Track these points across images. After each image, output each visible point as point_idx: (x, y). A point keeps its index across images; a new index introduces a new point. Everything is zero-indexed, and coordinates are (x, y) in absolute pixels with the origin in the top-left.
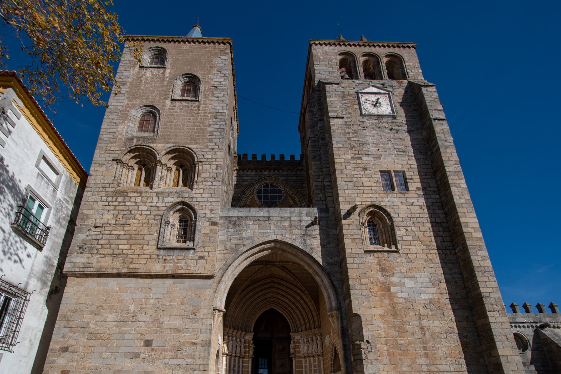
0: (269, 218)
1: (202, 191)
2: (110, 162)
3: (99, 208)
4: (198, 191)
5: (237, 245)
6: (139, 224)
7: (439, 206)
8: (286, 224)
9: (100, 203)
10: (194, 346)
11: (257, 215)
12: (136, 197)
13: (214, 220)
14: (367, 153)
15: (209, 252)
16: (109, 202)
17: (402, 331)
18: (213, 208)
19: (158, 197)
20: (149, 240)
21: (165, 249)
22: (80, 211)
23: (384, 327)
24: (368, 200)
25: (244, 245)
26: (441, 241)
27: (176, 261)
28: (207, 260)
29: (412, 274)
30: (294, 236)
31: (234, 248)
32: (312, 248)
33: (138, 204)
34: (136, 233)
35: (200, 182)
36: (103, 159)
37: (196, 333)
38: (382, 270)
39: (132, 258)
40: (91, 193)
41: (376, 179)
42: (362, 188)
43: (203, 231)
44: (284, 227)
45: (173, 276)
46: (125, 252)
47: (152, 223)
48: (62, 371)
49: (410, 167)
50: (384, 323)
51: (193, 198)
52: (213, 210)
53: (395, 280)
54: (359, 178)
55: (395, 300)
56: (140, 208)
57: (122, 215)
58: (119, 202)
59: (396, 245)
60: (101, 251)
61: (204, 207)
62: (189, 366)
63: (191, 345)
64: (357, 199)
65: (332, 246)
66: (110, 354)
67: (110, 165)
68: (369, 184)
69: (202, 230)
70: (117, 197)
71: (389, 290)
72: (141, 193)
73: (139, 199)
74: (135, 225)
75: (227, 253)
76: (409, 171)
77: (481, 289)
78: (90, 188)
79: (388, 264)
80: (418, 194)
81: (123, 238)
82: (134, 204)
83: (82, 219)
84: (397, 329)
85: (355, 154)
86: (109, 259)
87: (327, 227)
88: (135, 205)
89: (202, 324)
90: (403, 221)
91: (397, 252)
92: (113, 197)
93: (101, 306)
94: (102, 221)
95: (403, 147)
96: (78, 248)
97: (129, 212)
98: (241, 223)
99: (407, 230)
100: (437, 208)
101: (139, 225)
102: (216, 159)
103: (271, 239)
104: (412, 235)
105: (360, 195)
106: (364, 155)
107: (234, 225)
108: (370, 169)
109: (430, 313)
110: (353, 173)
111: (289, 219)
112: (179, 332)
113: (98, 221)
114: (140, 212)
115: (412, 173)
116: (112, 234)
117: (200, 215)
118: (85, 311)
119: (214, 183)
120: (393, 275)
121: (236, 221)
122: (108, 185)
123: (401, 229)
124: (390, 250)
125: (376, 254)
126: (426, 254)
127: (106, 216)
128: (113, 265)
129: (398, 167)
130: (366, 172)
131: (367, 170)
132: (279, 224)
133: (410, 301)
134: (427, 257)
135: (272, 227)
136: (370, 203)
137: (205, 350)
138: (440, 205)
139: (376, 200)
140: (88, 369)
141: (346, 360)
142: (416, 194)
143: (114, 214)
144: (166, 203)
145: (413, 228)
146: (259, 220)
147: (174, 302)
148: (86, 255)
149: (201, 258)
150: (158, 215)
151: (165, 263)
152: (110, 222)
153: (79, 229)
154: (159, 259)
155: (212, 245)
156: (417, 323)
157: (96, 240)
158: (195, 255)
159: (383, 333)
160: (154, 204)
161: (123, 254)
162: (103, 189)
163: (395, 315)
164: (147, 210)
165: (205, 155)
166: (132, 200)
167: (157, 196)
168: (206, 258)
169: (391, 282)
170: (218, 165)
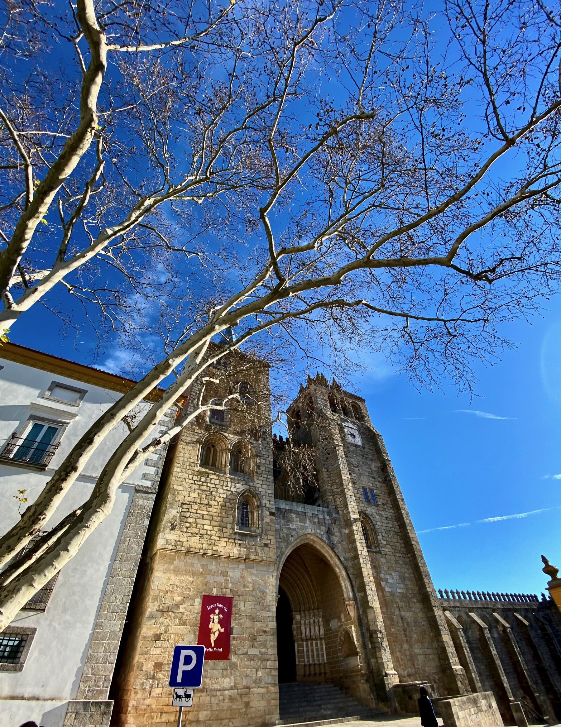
4: (259, 482)
5: (287, 535)
12: (215, 479)
15: (270, 540)
33: (217, 486)
34: (215, 514)
39: (215, 540)
46: (209, 532)
48: (155, 663)
51: (256, 487)
52: (270, 501)
53: (382, 576)
58: (203, 482)
59: (378, 546)
60: (190, 530)
62: (263, 656)
75: (281, 542)
83: (173, 494)
86: (196, 539)
89: (269, 611)
94: (189, 499)
113: (186, 498)
118: (174, 593)
119: (269, 477)
127: (192, 495)
128: (199, 546)
135: (308, 522)
138: (394, 518)
141: (364, 646)
147: (248, 587)
148: (177, 532)
149: (266, 545)
153: (170, 504)
154: (235, 543)
155: (272, 533)
157: (185, 517)
160: (228, 488)
161: (207, 534)
166: (213, 482)
168: (270, 546)
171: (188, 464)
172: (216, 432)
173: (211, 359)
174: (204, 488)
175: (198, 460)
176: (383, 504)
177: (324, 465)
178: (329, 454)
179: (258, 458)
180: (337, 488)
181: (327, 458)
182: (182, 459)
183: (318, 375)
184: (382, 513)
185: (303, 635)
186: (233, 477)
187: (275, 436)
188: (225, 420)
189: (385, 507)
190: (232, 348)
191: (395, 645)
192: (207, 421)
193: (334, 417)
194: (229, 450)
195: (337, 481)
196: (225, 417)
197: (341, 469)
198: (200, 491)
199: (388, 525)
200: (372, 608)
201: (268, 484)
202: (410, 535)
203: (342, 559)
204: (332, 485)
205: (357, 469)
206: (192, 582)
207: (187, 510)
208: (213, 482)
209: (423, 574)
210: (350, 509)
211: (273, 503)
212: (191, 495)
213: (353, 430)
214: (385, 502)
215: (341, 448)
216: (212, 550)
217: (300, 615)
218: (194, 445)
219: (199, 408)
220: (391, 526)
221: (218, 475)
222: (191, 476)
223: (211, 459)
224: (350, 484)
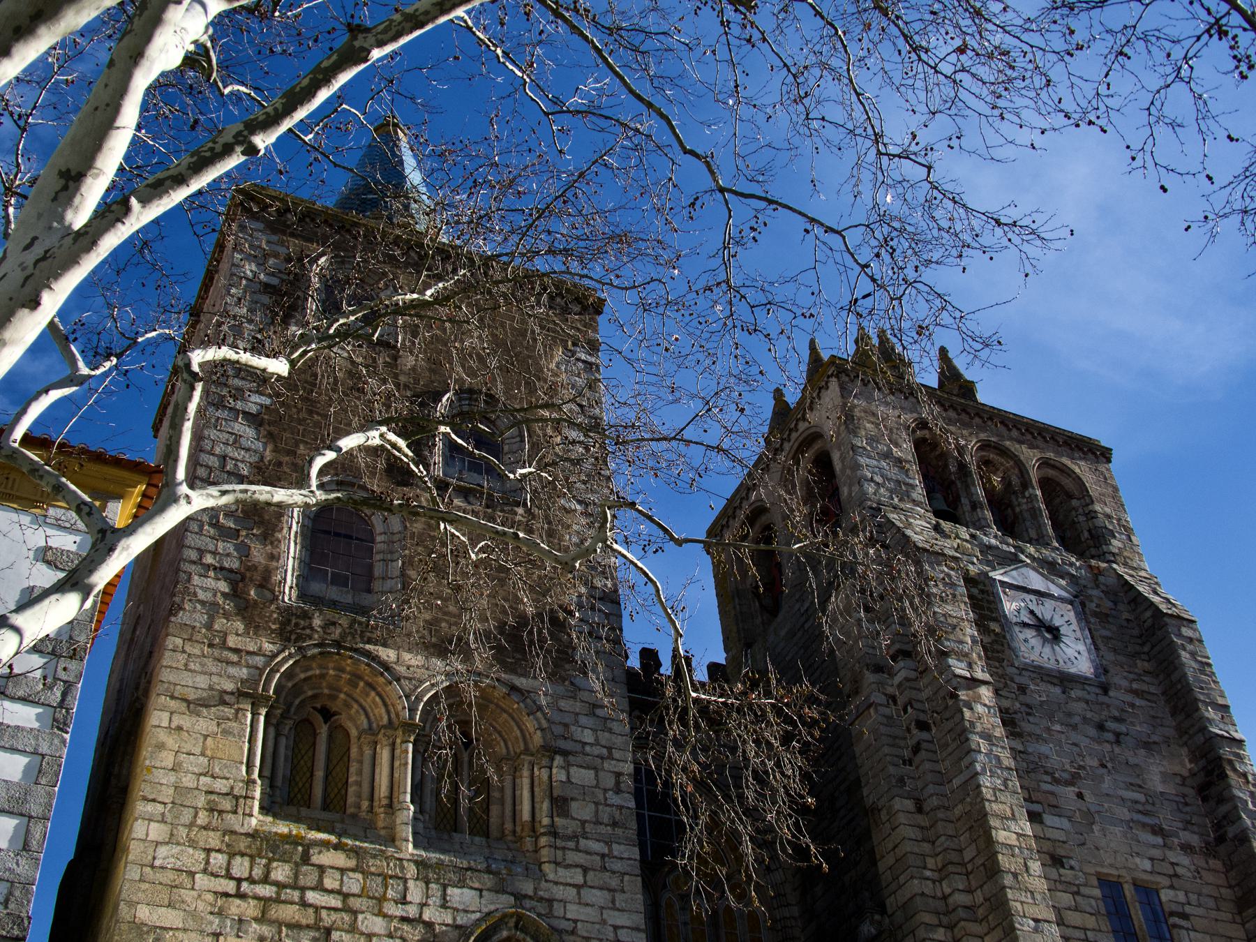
12: (342, 871)
14: (1053, 801)
16: (239, 881)
19: (427, 883)
33: (353, 902)
41: (1093, 902)
49: (1171, 872)
51: (550, 901)
58: (280, 886)
70: (270, 860)
73: (354, 883)
76: (1172, 887)
78: (160, 808)
82: (335, 902)
88: (339, 904)
92: (252, 857)
95: (1141, 798)
102: (610, 749)
108: (1072, 863)
115: (1181, 897)
119: (617, 849)
130: (1062, 871)
160: (412, 911)
165: (573, 728)
170: (618, 775)
171: (201, 801)
172: (337, 644)
173: (145, 201)
174: (289, 912)
175: (250, 782)
177: (901, 781)
178: (923, 726)
179: (558, 760)
180: (969, 891)
181: (916, 749)
182: (172, 778)
183: (862, 338)
186: (434, 856)
187: (650, 657)
188: (377, 586)
190: (263, 141)
192: (289, 593)
193: (948, 546)
194: (408, 727)
195: (968, 855)
196: (378, 570)
197: (987, 793)
198: (266, 930)
201: (614, 883)
204: (943, 873)
205: (1070, 791)
208: (329, 883)
213: (1049, 604)
215: (985, 693)
218: (229, 712)
219: (175, 499)
221: (356, 852)
222: (218, 860)
223: (320, 774)
224: (1035, 866)
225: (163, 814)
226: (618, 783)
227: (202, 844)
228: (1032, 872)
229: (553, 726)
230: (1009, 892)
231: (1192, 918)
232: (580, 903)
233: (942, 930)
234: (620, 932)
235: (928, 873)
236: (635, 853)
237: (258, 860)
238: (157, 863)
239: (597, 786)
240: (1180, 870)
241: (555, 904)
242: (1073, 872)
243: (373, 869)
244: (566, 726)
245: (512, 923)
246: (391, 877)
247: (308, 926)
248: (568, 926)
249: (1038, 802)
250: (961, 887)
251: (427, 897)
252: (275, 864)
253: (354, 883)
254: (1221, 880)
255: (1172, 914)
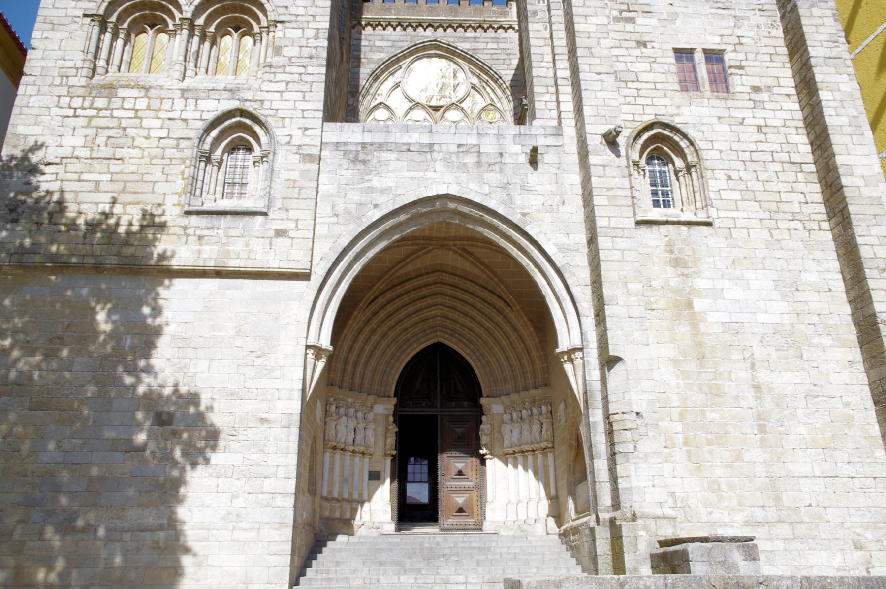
0: (431, 145)
1: (282, 86)
2: (76, 19)
3: (53, 122)
6: (143, 157)
7: (797, 128)
8: (470, 159)
9: (55, 111)
10: (266, 425)
11: (406, 139)
12: (136, 98)
13: (307, 150)
14: (647, 9)
15: (297, 220)
16: (75, 109)
17: (714, 393)
18: (308, 123)
19: (186, 99)
20: (165, 194)
21: (199, 213)
22: (10, 127)
23: (678, 384)
24: (648, 110)
25: (376, 206)
26: (800, 203)
27: (224, 241)
28: (293, 238)
29: (738, 273)
30: (487, 186)
31: (354, 211)
32: (524, 215)
33: (140, 114)
35: (280, 67)
36: (62, 13)
37: (269, 398)
38: (677, 263)
40: (36, 88)
41: (666, 67)
42: (636, 85)
43: (284, 175)
44: (464, 167)
45: (219, 274)
47: (170, 156)
49: (737, 41)
50: (677, 377)
52: (306, 129)
53: (701, 283)
54: (629, 64)
55: (702, 328)
56: (145, 123)
57: (105, 139)
58: (100, 110)
61: (287, 121)
63: (259, 424)
64: (625, 108)
65: (568, 208)
66: (80, 442)
67: (76, 26)
68: (650, 77)
69: (282, 171)
70: (94, 97)
71: (690, 305)
72: (147, 89)
73: (142, 104)
74: (133, 161)
76: (735, 51)
77: (875, 304)
78: (33, 78)
79: (688, 251)
80: (754, 101)
81: (108, 189)
82: (131, 114)
84: (706, 389)
85: (621, 12)
87: (559, 169)
88: (133, 116)
90: (722, 159)
91: (709, 224)
93: (59, 338)
94: (61, 152)
96: (7, 211)
97: (121, 131)
98: (369, 157)
99: (729, 178)
100: (794, 131)
101: (143, 161)
103: (435, 194)
104: (739, 188)
105: (628, 99)
106: (641, 14)
107: (355, 161)
109: (774, 354)
110: (615, 52)
111: (476, 149)
112: (232, 394)
114: (146, 131)
115: (741, 56)
116: (84, 181)
117: (278, 139)
120: (698, 274)
121: (358, 152)
122: (75, 71)
123: (717, 176)
124: (693, 218)
125: (663, 228)
126: (770, 229)
129: (713, 43)
130: (644, 50)
131: (645, 46)
132: (454, 158)
133: (733, 329)
134: (772, 236)
135: (439, 166)
136: (653, 117)
137: (289, 434)
139: (664, 112)
140: (33, 472)
142: (750, 100)
143: (86, 136)
144: (203, 111)
145: (742, 174)
146: (409, 150)
149: (280, 233)
150: (184, 139)
151: (201, 245)
152: (77, 153)
154: (188, 235)
155: (302, 204)
156: (746, 375)
158: (268, 227)
159: (674, 397)
162: (62, 80)
163: (701, 358)
164: (162, 128)
165: (290, 8)
166: (126, 105)
167: (182, 96)
168: (292, 234)
169: (694, 289)
170: (318, 29)
176: (756, 89)
184: (747, 114)
185: (506, 443)
189: (765, 96)
191: (711, 453)
198: (88, 131)
199: (761, 147)
200: (617, 360)
201: (306, 88)
202: (839, 160)
203: (551, 250)
206: (69, 325)
207: (54, 177)
209: (866, 264)
210: (587, 111)
211: (318, 132)
212: (63, 143)
214: (770, 82)
216: (118, 254)
217: (502, 403)
220: (776, 147)
222: (65, 101)
225: (35, 81)
226: (317, 33)
227: (56, 94)
228: (602, 46)
229: (278, 9)
230: (580, 60)
231: (746, 68)
232: (282, 100)
233: (548, 95)
234: (305, 113)
235: (543, 64)
236: (323, 70)
237: (87, 98)
238: (30, 105)
239: (303, 37)
240: (743, 40)
241: (265, 103)
242: (653, 50)
243: (154, 96)
244: (286, 7)
245: (238, 113)
246: (164, 99)
247: (113, 128)
248: (272, 112)
249: (634, 11)
250: (561, 67)
251: (186, 106)
252: (96, 99)
253: (142, 104)
254: (781, 42)
255: (730, 67)
